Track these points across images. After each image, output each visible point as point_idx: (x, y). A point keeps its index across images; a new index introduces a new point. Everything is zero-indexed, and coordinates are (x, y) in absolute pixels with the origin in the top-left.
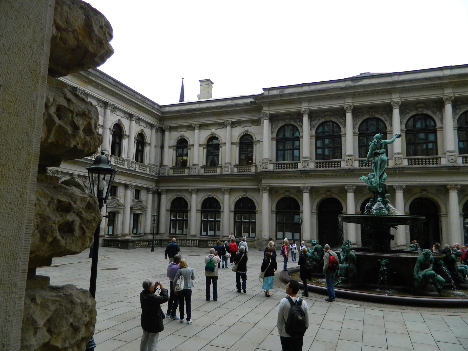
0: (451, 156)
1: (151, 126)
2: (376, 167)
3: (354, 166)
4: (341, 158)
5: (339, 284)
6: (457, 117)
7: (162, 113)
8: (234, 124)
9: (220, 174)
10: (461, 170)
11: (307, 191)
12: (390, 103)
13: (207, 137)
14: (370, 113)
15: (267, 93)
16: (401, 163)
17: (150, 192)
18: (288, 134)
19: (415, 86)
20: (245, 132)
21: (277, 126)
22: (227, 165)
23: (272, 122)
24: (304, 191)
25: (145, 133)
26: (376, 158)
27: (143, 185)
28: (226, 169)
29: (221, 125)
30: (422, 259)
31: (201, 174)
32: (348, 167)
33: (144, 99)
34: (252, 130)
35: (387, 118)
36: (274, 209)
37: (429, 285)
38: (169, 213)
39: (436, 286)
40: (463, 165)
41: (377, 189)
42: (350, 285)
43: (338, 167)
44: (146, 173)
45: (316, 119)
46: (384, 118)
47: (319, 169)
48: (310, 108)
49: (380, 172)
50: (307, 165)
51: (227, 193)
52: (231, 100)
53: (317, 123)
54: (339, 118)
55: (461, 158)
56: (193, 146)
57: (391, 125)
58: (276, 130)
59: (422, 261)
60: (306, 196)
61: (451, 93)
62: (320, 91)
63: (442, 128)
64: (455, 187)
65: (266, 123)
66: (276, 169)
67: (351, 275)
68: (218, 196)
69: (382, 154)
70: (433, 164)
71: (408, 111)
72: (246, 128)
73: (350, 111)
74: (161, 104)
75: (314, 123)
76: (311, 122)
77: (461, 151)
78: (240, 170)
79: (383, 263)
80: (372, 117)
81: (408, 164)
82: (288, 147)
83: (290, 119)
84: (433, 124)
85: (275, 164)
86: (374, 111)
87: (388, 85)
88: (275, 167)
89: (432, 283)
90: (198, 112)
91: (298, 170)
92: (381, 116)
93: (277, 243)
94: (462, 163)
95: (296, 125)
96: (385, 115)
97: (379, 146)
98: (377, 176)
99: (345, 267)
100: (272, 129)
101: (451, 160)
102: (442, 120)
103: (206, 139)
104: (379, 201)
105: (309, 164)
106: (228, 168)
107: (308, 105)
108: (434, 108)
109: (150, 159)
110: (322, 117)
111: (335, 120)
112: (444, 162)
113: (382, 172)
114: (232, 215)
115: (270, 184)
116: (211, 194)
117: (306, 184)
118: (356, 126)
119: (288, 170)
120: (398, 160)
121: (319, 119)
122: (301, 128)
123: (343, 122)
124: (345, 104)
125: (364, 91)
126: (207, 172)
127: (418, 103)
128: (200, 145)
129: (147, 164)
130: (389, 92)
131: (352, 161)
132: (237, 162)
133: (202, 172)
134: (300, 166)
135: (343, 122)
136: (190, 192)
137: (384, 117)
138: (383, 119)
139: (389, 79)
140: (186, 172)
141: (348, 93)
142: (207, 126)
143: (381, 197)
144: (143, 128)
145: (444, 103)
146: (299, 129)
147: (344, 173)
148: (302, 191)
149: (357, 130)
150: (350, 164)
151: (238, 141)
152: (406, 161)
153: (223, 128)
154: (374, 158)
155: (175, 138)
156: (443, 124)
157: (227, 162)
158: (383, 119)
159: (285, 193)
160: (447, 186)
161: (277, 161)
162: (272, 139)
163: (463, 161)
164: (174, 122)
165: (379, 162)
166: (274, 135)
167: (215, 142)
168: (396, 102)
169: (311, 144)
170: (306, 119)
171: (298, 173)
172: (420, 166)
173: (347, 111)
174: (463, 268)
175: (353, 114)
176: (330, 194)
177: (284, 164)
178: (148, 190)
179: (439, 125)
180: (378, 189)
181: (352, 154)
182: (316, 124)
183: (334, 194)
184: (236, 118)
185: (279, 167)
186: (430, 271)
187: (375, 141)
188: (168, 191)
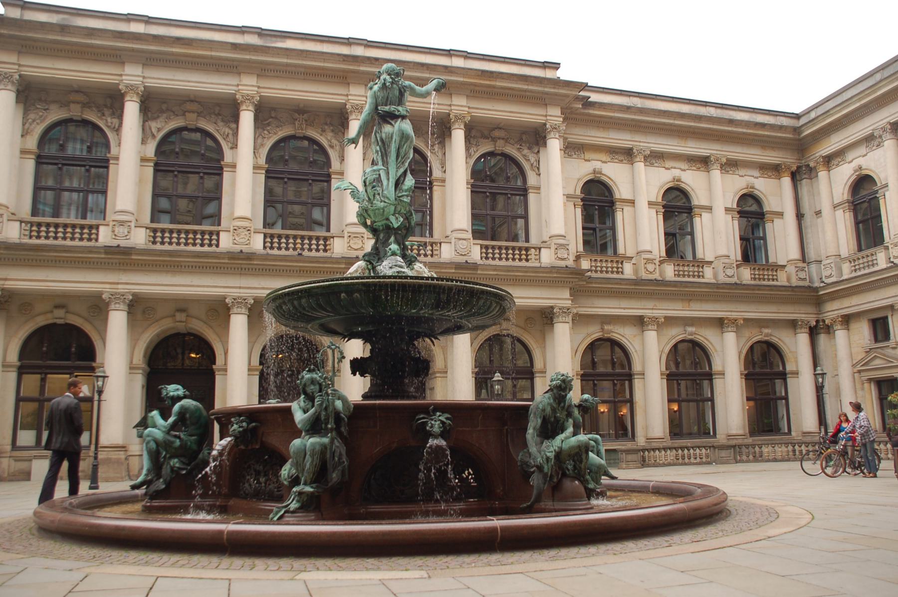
0: (461, 241)
2: (385, 155)
3: (251, 246)
4: (219, 225)
5: (293, 512)
10: (479, 272)
11: (122, 307)
14: (297, 123)
18: (75, 149)
21: (43, 120)
23: (25, 104)
24: (112, 306)
26: (387, 129)
30: (548, 404)
32: (238, 248)
35: (334, 142)
41: (388, 219)
43: (210, 245)
45: (158, 117)
47: (158, 247)
48: (145, 80)
49: (398, 168)
50: (126, 234)
53: (162, 126)
54: (221, 124)
58: (39, 129)
59: (548, 409)
60: (118, 320)
62: (179, 40)
63: (444, 181)
66: (31, 237)
67: (334, 475)
69: (403, 117)
73: (251, 108)
75: (154, 125)
76: (144, 122)
77: (477, 234)
80: (300, 133)
82: (71, 182)
83: (85, 105)
85: (27, 223)
87: (344, 61)
88: (27, 233)
91: (97, 244)
92: (321, 135)
93: (16, 461)
95: (101, 124)
96: (330, 135)
97: (397, 93)
98: (388, 179)
99: (318, 448)
100: (24, 125)
101: (463, 250)
102: (443, 165)
104: (394, 254)
105: (132, 232)
107: (143, 73)
111: (210, 128)
115: (6, 279)
117: (120, 286)
118: (261, 150)
119: (68, 243)
121: (168, 118)
122: (115, 133)
123: (230, 136)
124: (240, 87)
125: (287, 65)
131: (247, 233)
134: (105, 237)
135: (230, 136)
138: (325, 143)
139: (345, 50)
141: (249, 61)
143: (397, 242)
145: (450, 128)
146: (110, 135)
147: (227, 261)
148: (107, 304)
149: (262, 161)
150: (242, 240)
154: (380, 128)
156: (445, 172)
159: (52, 312)
162: (24, 152)
165: (396, 137)
166: (32, 143)
168: (357, 105)
169: (141, 181)
170: (131, 110)
171: (99, 253)
173: (244, 107)
175: (256, 119)
176: (184, 319)
177: (57, 226)
180: (392, 219)
181: (249, 215)
182: (159, 130)
183: (194, 320)
185: (39, 232)
186: (568, 439)
187: (385, 80)
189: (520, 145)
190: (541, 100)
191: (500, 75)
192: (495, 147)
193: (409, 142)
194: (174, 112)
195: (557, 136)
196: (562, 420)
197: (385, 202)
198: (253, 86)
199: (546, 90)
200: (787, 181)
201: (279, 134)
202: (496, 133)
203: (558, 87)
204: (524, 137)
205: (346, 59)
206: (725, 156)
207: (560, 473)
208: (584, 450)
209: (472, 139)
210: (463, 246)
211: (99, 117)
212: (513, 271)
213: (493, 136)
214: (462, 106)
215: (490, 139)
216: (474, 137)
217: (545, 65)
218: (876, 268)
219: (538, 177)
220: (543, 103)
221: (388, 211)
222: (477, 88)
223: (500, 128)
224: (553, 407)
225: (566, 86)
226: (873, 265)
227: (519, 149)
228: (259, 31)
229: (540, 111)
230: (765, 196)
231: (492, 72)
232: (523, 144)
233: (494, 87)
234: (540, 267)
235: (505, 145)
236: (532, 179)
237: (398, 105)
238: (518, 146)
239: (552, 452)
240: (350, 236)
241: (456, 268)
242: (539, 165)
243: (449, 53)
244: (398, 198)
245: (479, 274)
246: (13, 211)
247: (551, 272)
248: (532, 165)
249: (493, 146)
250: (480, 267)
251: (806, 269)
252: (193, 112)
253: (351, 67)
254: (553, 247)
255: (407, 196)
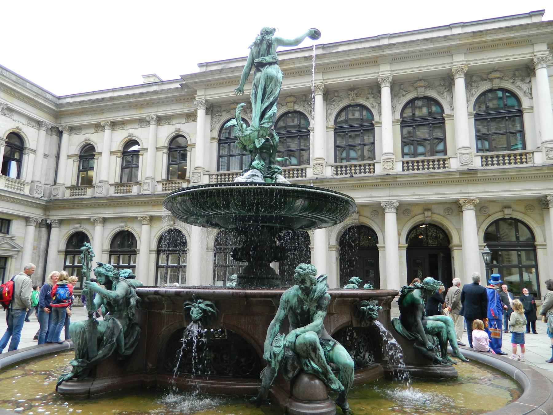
0: (464, 155)
1: (39, 123)
6: (474, 99)
7: (57, 105)
8: (160, 120)
9: (136, 194)
10: (479, 175)
12: (377, 79)
13: (122, 141)
14: (350, 97)
15: (203, 69)
16: (392, 168)
17: (32, 224)
19: (412, 52)
20: (176, 131)
22: (147, 181)
25: (24, 133)
27: (14, 211)
28: (146, 187)
29: (143, 122)
30: (294, 295)
31: (109, 195)
33: (21, 81)
34: (185, 128)
35: (375, 104)
36: (212, 244)
37: (306, 379)
38: (63, 257)
39: (326, 383)
40: (482, 168)
42: (98, 385)
44: (21, 192)
46: (369, 105)
51: (146, 223)
52: (158, 85)
55: (480, 158)
56: (101, 153)
57: (380, 114)
59: (294, 301)
61: (463, 61)
63: (453, 116)
64: (471, 202)
65: (201, 113)
67: (100, 352)
68: (132, 228)
70: (439, 168)
71: (404, 93)
72: (178, 126)
74: (58, 95)
78: (166, 187)
79: (195, 313)
80: (353, 103)
81: (403, 170)
84: (439, 110)
86: (356, 94)
87: (373, 51)
89: (315, 375)
90: (108, 103)
94: (480, 165)
96: (371, 100)
97: (265, 46)
102: (451, 105)
103: (121, 143)
106: (149, 185)
108: (441, 88)
109: (33, 173)
110: (283, 106)
111: (301, 109)
112: (454, 165)
113: (266, 104)
114: (153, 256)
116: (123, 224)
120: (388, 163)
125: (339, 62)
126: (122, 191)
127: (418, 81)
128: (112, 153)
129: (29, 180)
130: (375, 62)
132: (164, 177)
133: (112, 192)
136: (92, 222)
137: (370, 103)
138: (369, 106)
140: (89, 193)
142: (124, 124)
143: (262, 158)
144: (21, 126)
149: (332, 123)
150: (318, 172)
151: (166, 144)
152: (401, 164)
153: (146, 126)
155: (78, 143)
156: (453, 109)
157: (147, 176)
158: (368, 105)
160: (460, 200)
161: (218, 170)
162: (212, 139)
163: (482, 162)
164: (75, 119)
165: (263, 81)
167: (135, 148)
172: (421, 171)
174: (441, 324)
178: (27, 220)
179: (447, 111)
180: (256, 141)
184: (162, 111)
188: (61, 222)
189: (514, 80)
190: (528, 42)
191: (489, 32)
192: (493, 85)
193: (273, 82)
194: (281, 104)
195: (545, 66)
196: (311, 313)
197: (252, 130)
198: (320, 80)
199: (531, 33)
201: (341, 105)
202: (493, 75)
203: (541, 28)
204: (517, 73)
205: (374, 49)
207: (299, 367)
208: (310, 348)
209: (473, 83)
210: (466, 158)
211: (245, 115)
212: (508, 172)
213: (490, 78)
214: (461, 61)
215: (488, 80)
216: (475, 81)
217: (531, 15)
219: (531, 100)
220: (531, 43)
221: (253, 136)
222: (472, 46)
223: (496, 71)
224: (300, 298)
225: (549, 26)
227: (513, 83)
228: (322, 46)
229: (529, 50)
231: (481, 31)
232: (516, 79)
233: (485, 42)
234: (534, 167)
235: (500, 83)
236: (525, 103)
237: (267, 55)
238: (512, 81)
239: (279, 347)
240: (384, 161)
241: (460, 174)
242: (531, 91)
243: (449, 27)
244: (261, 127)
245: (479, 177)
246: (208, 170)
247: (542, 169)
248: (525, 92)
249: (491, 85)
250: (479, 172)
252: (291, 102)
253: (378, 54)
254: (544, 150)
255: (268, 122)
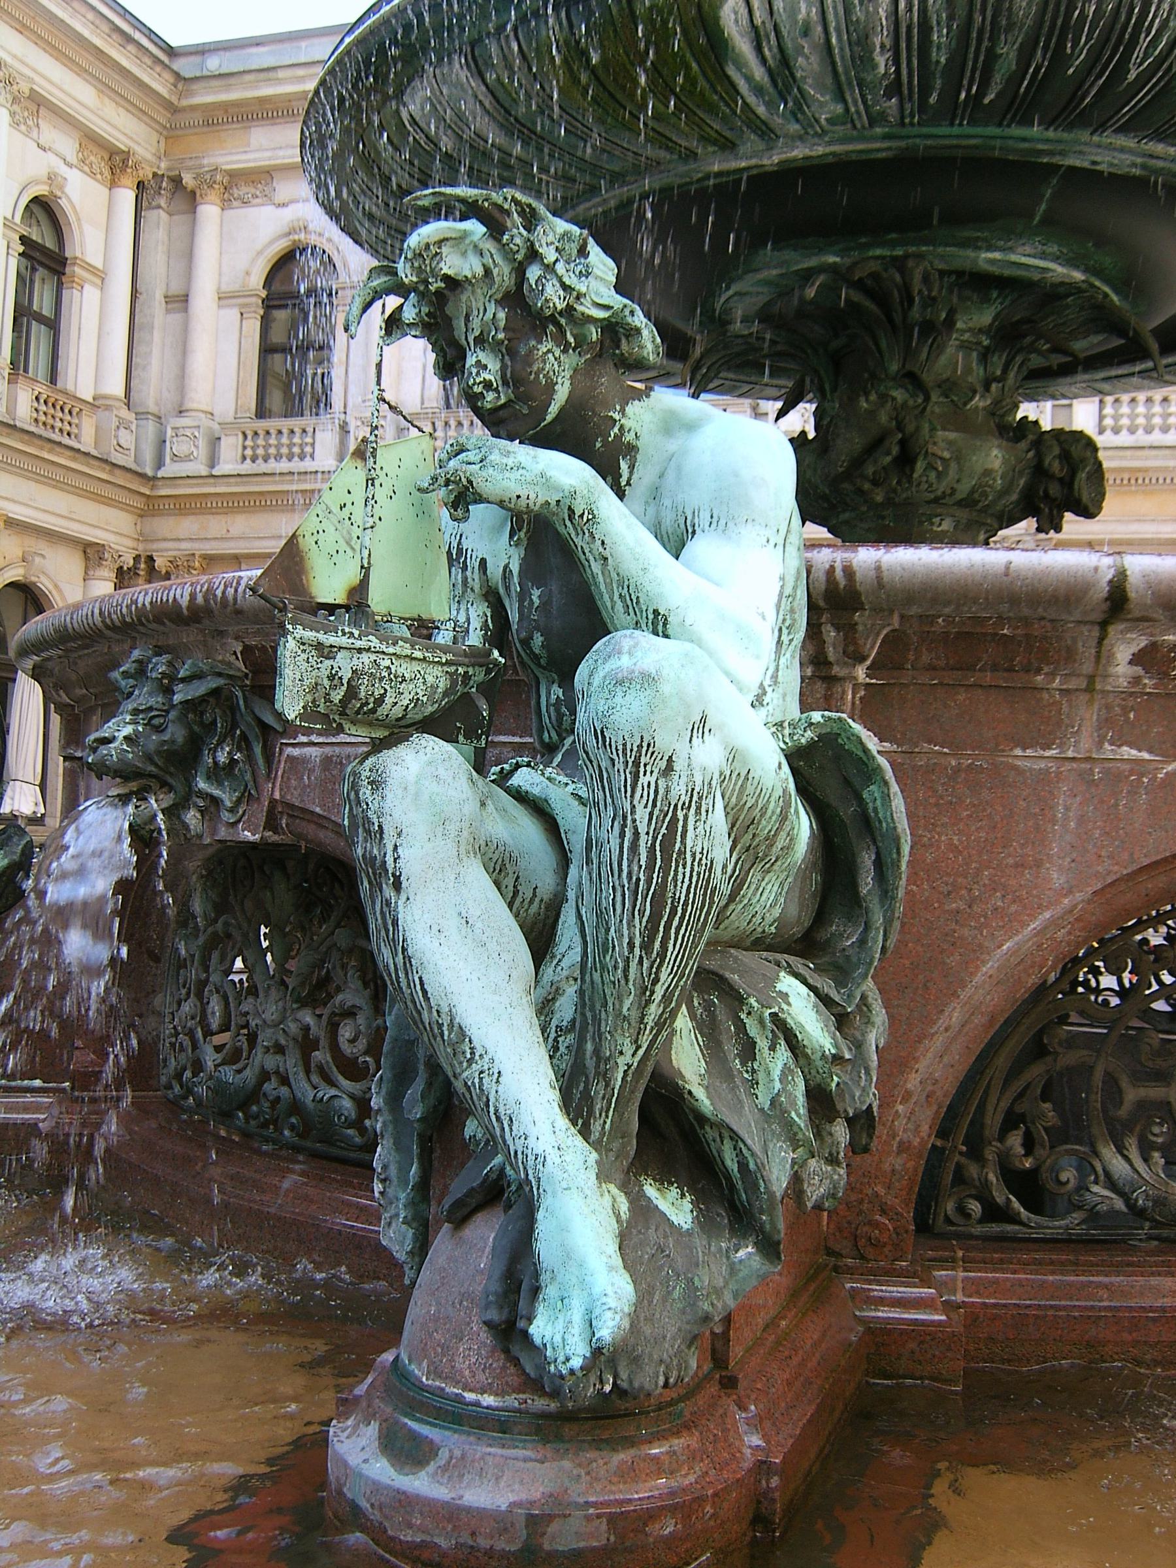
200: (126, 197)
206: (32, 81)
218: (308, 465)
226: (302, 457)
230: (79, 220)
251: (133, 427)
